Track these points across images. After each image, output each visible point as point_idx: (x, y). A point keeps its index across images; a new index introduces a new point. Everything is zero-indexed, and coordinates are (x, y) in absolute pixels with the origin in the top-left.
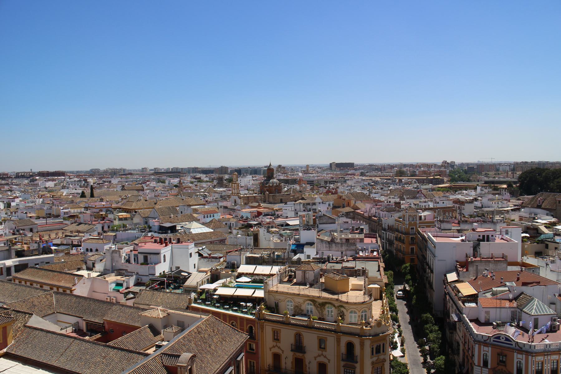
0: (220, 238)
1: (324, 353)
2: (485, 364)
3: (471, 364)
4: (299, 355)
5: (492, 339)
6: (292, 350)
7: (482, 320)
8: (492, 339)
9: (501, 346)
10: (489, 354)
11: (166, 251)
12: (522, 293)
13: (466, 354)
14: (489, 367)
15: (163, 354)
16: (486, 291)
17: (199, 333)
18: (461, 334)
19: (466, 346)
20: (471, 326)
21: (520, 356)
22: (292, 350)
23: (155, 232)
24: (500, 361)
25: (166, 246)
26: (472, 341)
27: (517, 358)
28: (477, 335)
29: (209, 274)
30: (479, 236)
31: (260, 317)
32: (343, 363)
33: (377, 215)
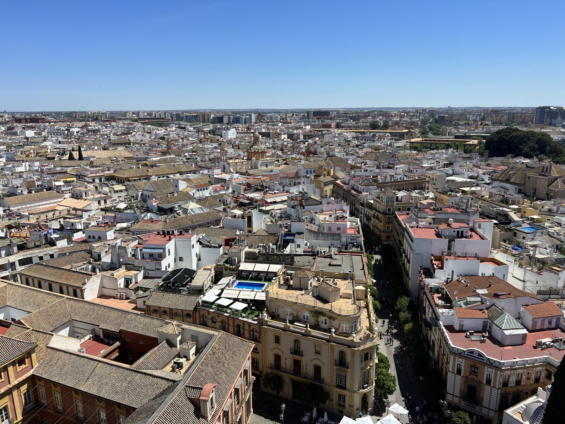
0: (216, 218)
1: (319, 358)
2: (459, 372)
3: (446, 369)
4: (297, 357)
5: (466, 353)
7: (457, 328)
8: (466, 353)
9: (474, 360)
11: (170, 246)
12: (493, 304)
13: (441, 356)
14: (462, 375)
15: (186, 386)
17: (214, 353)
18: (437, 337)
20: (448, 337)
21: (490, 370)
23: (153, 213)
25: (170, 240)
26: (447, 351)
27: (487, 371)
28: (453, 348)
29: (213, 272)
30: (454, 231)
31: (261, 322)
32: (335, 367)
33: (355, 187)
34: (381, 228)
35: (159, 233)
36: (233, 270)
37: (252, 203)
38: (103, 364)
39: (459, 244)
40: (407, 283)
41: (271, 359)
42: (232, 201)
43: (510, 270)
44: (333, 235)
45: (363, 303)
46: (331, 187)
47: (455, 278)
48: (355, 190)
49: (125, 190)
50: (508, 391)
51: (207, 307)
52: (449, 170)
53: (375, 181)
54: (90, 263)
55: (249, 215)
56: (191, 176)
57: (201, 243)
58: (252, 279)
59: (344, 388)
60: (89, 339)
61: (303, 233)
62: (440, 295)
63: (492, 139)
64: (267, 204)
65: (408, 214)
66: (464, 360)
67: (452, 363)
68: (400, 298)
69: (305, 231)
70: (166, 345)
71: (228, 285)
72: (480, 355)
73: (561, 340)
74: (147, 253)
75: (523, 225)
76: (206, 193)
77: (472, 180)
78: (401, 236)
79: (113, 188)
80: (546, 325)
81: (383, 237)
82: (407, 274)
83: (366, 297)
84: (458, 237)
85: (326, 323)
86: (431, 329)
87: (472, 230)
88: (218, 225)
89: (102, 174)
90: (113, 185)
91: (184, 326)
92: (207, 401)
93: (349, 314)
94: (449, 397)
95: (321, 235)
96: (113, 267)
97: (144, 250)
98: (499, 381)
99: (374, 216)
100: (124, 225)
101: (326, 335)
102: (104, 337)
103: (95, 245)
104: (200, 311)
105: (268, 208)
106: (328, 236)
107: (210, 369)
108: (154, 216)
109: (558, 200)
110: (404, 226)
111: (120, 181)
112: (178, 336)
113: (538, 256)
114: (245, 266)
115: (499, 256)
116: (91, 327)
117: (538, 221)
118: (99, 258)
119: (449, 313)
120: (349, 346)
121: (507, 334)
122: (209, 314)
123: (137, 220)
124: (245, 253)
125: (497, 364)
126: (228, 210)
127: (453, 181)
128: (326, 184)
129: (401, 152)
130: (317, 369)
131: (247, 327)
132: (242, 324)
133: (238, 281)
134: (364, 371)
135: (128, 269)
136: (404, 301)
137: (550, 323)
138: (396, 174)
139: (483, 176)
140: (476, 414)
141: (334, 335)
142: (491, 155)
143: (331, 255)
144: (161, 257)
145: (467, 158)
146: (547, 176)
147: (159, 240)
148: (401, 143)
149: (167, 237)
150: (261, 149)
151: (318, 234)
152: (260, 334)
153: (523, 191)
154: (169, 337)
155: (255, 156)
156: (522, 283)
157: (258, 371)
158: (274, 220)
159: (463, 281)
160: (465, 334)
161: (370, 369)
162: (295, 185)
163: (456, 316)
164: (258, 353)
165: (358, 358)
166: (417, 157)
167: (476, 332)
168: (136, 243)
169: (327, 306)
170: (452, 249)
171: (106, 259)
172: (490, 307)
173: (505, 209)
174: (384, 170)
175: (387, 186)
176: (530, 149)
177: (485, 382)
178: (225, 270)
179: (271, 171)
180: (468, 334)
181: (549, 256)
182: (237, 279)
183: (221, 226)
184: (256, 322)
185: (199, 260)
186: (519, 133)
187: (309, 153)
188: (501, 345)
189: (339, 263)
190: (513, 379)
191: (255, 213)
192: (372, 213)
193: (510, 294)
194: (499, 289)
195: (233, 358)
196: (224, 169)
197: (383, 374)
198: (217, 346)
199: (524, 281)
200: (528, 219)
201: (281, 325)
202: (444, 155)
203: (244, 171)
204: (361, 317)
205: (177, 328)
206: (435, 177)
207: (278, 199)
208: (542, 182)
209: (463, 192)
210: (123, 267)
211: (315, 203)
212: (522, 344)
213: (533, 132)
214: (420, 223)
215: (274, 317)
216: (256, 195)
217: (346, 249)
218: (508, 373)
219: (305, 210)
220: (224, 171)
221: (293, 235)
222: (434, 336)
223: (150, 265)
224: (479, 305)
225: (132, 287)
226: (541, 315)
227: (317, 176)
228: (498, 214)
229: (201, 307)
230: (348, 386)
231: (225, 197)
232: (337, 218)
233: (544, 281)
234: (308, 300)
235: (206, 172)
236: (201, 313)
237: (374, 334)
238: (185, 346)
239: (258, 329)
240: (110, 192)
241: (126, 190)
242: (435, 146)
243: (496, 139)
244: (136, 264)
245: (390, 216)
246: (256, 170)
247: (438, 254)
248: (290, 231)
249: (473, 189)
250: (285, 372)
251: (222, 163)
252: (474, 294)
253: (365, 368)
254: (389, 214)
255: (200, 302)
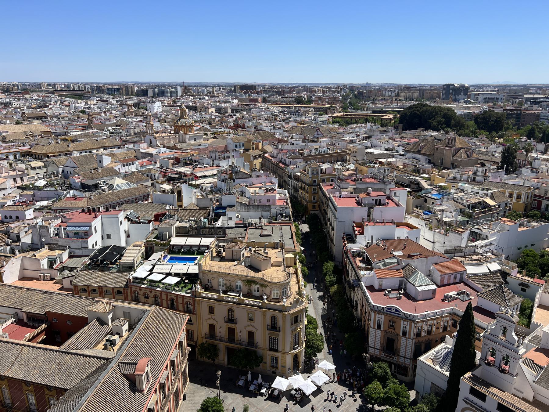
0: (145, 194)
1: (252, 324)
2: (379, 327)
3: (368, 325)
4: (231, 325)
5: (385, 309)
6: (225, 322)
7: (377, 287)
8: (385, 309)
10: (382, 320)
11: (97, 223)
12: (408, 265)
13: (364, 314)
14: (382, 329)
15: (120, 363)
16: (379, 262)
17: (148, 328)
18: (359, 297)
19: (364, 308)
20: (369, 297)
22: (225, 322)
23: (77, 190)
24: (391, 326)
25: (96, 217)
26: (368, 309)
27: (404, 324)
28: (374, 306)
29: (143, 248)
31: (195, 295)
32: (268, 332)
33: (283, 160)
34: (308, 199)
35: (83, 211)
36: (164, 245)
37: (181, 178)
38: (28, 348)
39: (377, 211)
40: (332, 249)
41: (206, 329)
42: (161, 176)
43: (422, 233)
44: (264, 207)
45: (292, 270)
46: (260, 160)
47: (375, 242)
48: (283, 163)
49: (43, 166)
50: (420, 341)
51: (139, 283)
52: (368, 143)
53: (301, 154)
54: (8, 245)
55: (179, 189)
56: (115, 151)
57: (129, 220)
58: (184, 253)
59: (276, 351)
60: (12, 323)
61: (234, 206)
62: (361, 258)
63: (405, 114)
64: (197, 178)
65: (331, 185)
66: (383, 316)
67: (373, 320)
68: (326, 263)
69: (236, 205)
70: (97, 323)
71: (159, 260)
72: (397, 310)
73: (464, 292)
74: (72, 232)
75: (432, 192)
76: (133, 169)
77: (388, 152)
78: (325, 206)
79: (30, 165)
80: (452, 280)
81: (310, 207)
82: (332, 241)
83: (295, 264)
84: (376, 204)
85: (258, 291)
86: (354, 290)
87: (389, 198)
88: (146, 200)
89: (17, 150)
90: (29, 161)
91: (115, 303)
92: (143, 375)
93: (279, 281)
94: (371, 350)
95: (251, 207)
96: (34, 247)
97: (68, 229)
98: (414, 332)
99: (301, 188)
100: (45, 203)
101: (258, 302)
102: (30, 321)
103: (12, 225)
104: (131, 288)
105: (198, 182)
106: (258, 208)
107: (144, 343)
108: (77, 194)
109: (462, 169)
110: (329, 196)
111: (37, 157)
112: (109, 313)
113: (445, 219)
114: (176, 241)
115: (413, 221)
116: (13, 311)
117: (445, 188)
118: (18, 239)
119: (369, 274)
120: (280, 311)
121: (419, 290)
122: (141, 290)
123: (58, 198)
124: (177, 228)
125: (412, 317)
126: (157, 185)
127: (371, 153)
128: (255, 158)
129: (325, 126)
130: (251, 335)
131: (180, 300)
132: (175, 298)
133: (169, 256)
134: (294, 333)
135: (51, 249)
136: (329, 266)
137: (455, 278)
138: (320, 147)
139: (398, 148)
140: (394, 363)
141: (266, 301)
142: (405, 129)
143: (262, 226)
144: (87, 235)
145: (383, 131)
146: (451, 147)
147: (84, 218)
148: (324, 118)
149: (93, 215)
150: (188, 122)
151: (248, 206)
152: (194, 306)
153: (432, 162)
154: (100, 316)
155: (183, 129)
156: (432, 244)
157: (194, 341)
158: (204, 194)
159: (381, 245)
160: (383, 293)
161: (300, 330)
162: (224, 159)
163: (376, 277)
164: (192, 324)
165: (288, 322)
166: (339, 130)
167: (393, 290)
168: (59, 221)
169: (259, 275)
170: (371, 215)
171: (26, 239)
172: (405, 267)
173: (417, 178)
174: (309, 144)
175: (312, 159)
176: (438, 122)
177: (401, 334)
178: (156, 245)
179: (200, 145)
180: (387, 292)
181: (454, 219)
182: (169, 254)
183: (150, 201)
184: (189, 295)
185: (128, 236)
186: (429, 108)
187: (237, 127)
188: (414, 300)
189: (269, 234)
190: (425, 330)
191: (184, 187)
192: (299, 184)
193: (421, 255)
194: (413, 250)
195: (167, 331)
196: (151, 143)
197: (312, 335)
198: (151, 321)
199: (433, 242)
200: (436, 187)
201: (215, 295)
202: (363, 129)
203: (171, 145)
204: (291, 283)
205: (108, 305)
206: (355, 150)
207: (208, 173)
208: (448, 153)
209: (381, 163)
210: (46, 247)
211: (245, 176)
212: (432, 299)
213: (440, 107)
214: (343, 193)
215: (207, 288)
216: (185, 170)
217: (276, 219)
218: (421, 324)
219: (235, 183)
220: (150, 145)
221: (225, 208)
222: (357, 296)
223: (76, 244)
224: (396, 266)
225: (57, 267)
226: (447, 272)
227: (246, 150)
228: (411, 182)
229: (132, 284)
230: (280, 348)
231: (153, 172)
232: (267, 191)
233: (450, 242)
234: (241, 270)
235: (131, 146)
236: (133, 289)
237: (303, 298)
238: (117, 323)
239: (192, 301)
240: (27, 169)
241: (45, 166)
242: (356, 120)
243: (408, 114)
244: (60, 244)
245: (315, 187)
246: (185, 144)
247: (359, 221)
248: (222, 205)
249: (389, 160)
250: (220, 340)
251: (148, 137)
252: (391, 256)
253: (295, 329)
254: (314, 186)
255: (131, 278)
